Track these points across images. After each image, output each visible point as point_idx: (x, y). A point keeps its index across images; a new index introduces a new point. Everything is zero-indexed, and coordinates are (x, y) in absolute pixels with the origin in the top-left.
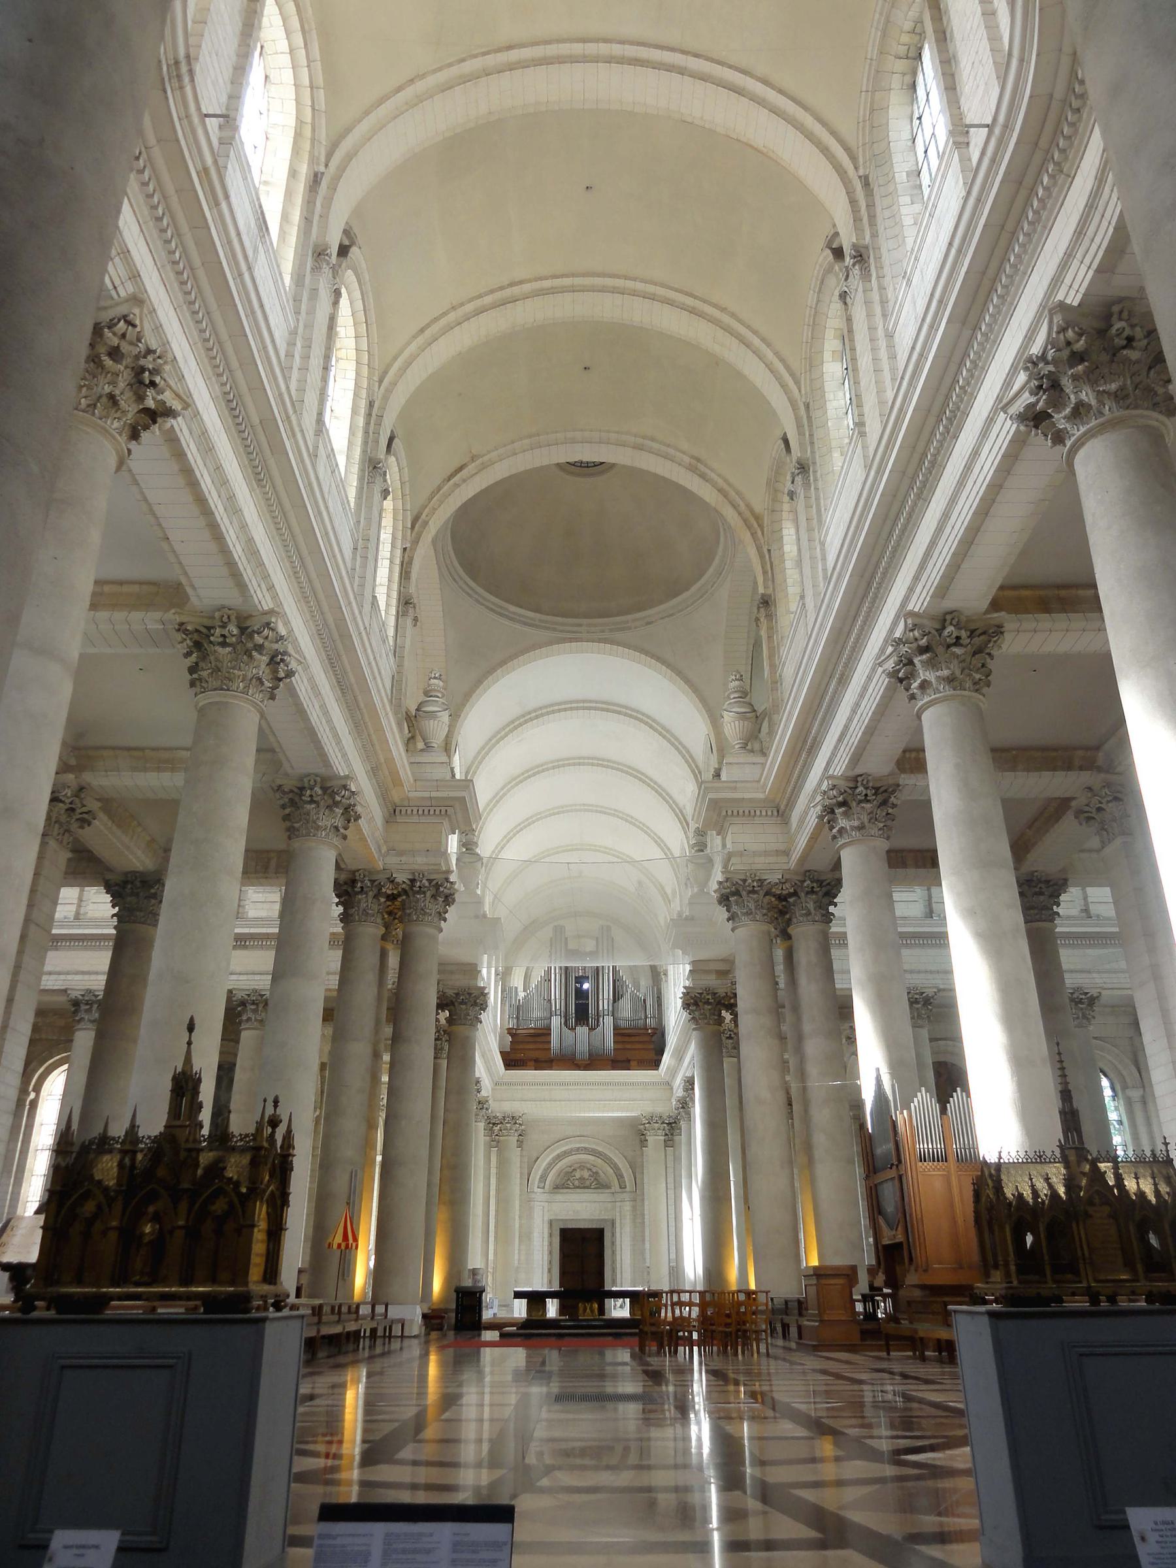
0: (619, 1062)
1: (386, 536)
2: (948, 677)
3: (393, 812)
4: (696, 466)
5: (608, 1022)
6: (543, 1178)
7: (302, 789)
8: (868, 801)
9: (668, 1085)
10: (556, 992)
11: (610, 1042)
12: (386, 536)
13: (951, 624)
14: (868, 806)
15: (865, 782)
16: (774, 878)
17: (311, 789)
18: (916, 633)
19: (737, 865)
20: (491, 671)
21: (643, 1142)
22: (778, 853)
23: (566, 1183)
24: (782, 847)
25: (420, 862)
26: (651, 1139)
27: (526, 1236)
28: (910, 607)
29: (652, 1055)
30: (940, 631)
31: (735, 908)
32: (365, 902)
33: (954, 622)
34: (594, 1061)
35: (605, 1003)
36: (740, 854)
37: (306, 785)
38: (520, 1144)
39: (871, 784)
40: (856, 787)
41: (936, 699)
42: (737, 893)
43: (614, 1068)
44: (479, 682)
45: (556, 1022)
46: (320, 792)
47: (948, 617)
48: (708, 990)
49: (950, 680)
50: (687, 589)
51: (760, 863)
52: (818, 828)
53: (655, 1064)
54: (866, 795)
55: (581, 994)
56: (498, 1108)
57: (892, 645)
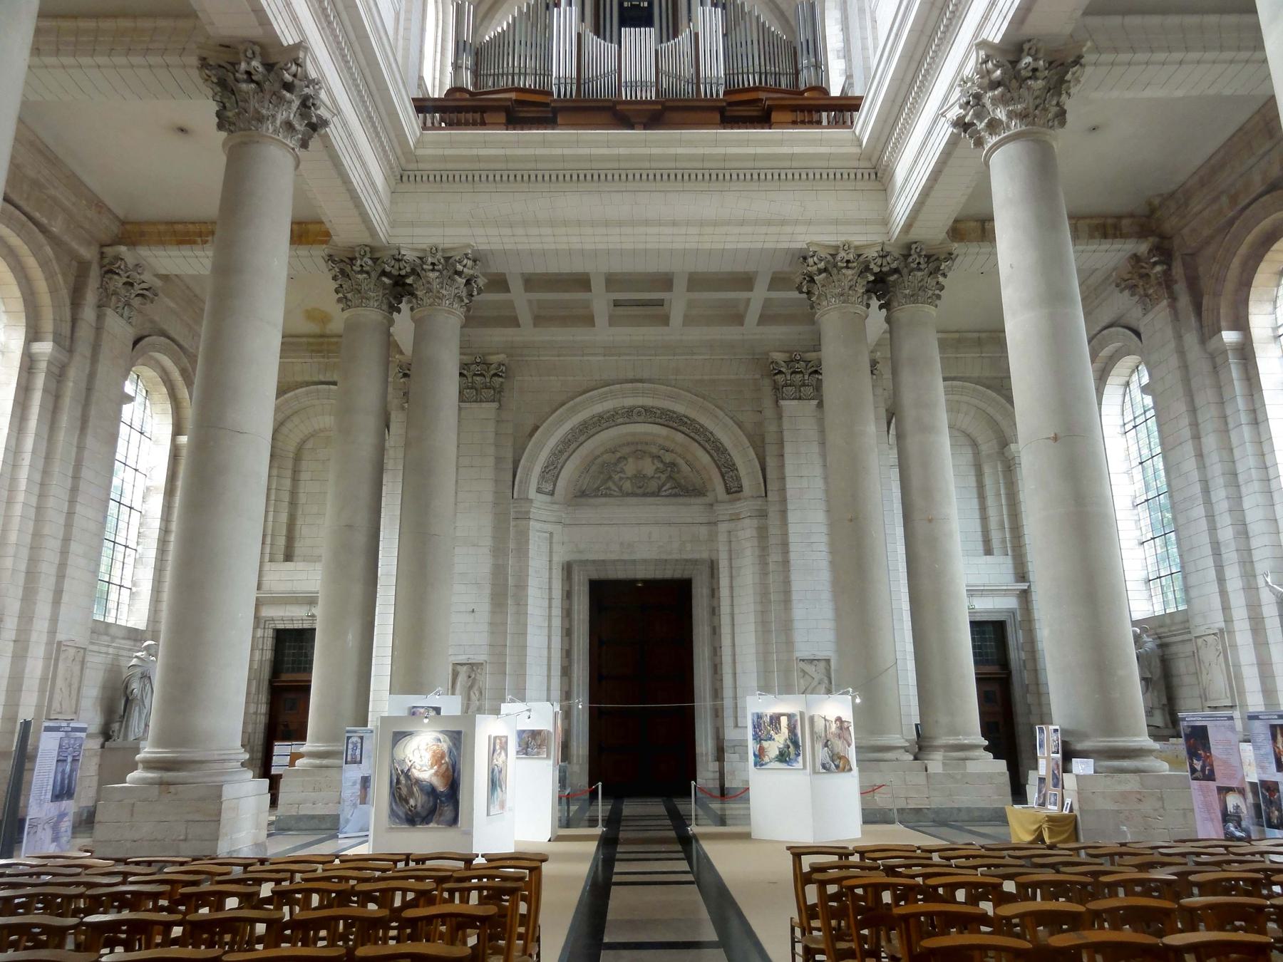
2: (1020, 114)
7: (352, 259)
8: (920, 270)
13: (1029, 54)
14: (919, 274)
15: (918, 250)
17: (362, 260)
18: (990, 65)
28: (984, 36)
30: (1014, 63)
33: (1033, 52)
37: (357, 255)
39: (923, 253)
40: (910, 255)
41: (1005, 138)
46: (370, 262)
47: (1026, 47)
49: (1023, 116)
54: (919, 263)
57: (960, 85)
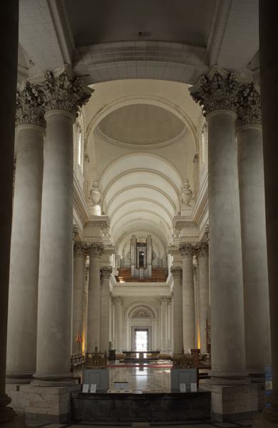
0: (153, 280)
1: (80, 143)
3: (86, 225)
4: (176, 108)
5: (150, 267)
6: (129, 314)
9: (168, 286)
10: (133, 257)
11: (150, 274)
12: (80, 143)
16: (194, 245)
19: (184, 240)
20: (111, 163)
21: (161, 304)
22: (196, 237)
23: (136, 315)
24: (197, 235)
25: (94, 240)
26: (163, 303)
27: (124, 331)
29: (163, 277)
31: (184, 253)
32: (79, 251)
34: (145, 279)
35: (149, 260)
36: (185, 237)
38: (122, 304)
42: (184, 248)
43: (152, 282)
44: (107, 167)
45: (133, 267)
48: (178, 267)
50: (174, 137)
51: (190, 240)
52: (204, 236)
53: (165, 280)
55: (141, 257)
56: (116, 294)
